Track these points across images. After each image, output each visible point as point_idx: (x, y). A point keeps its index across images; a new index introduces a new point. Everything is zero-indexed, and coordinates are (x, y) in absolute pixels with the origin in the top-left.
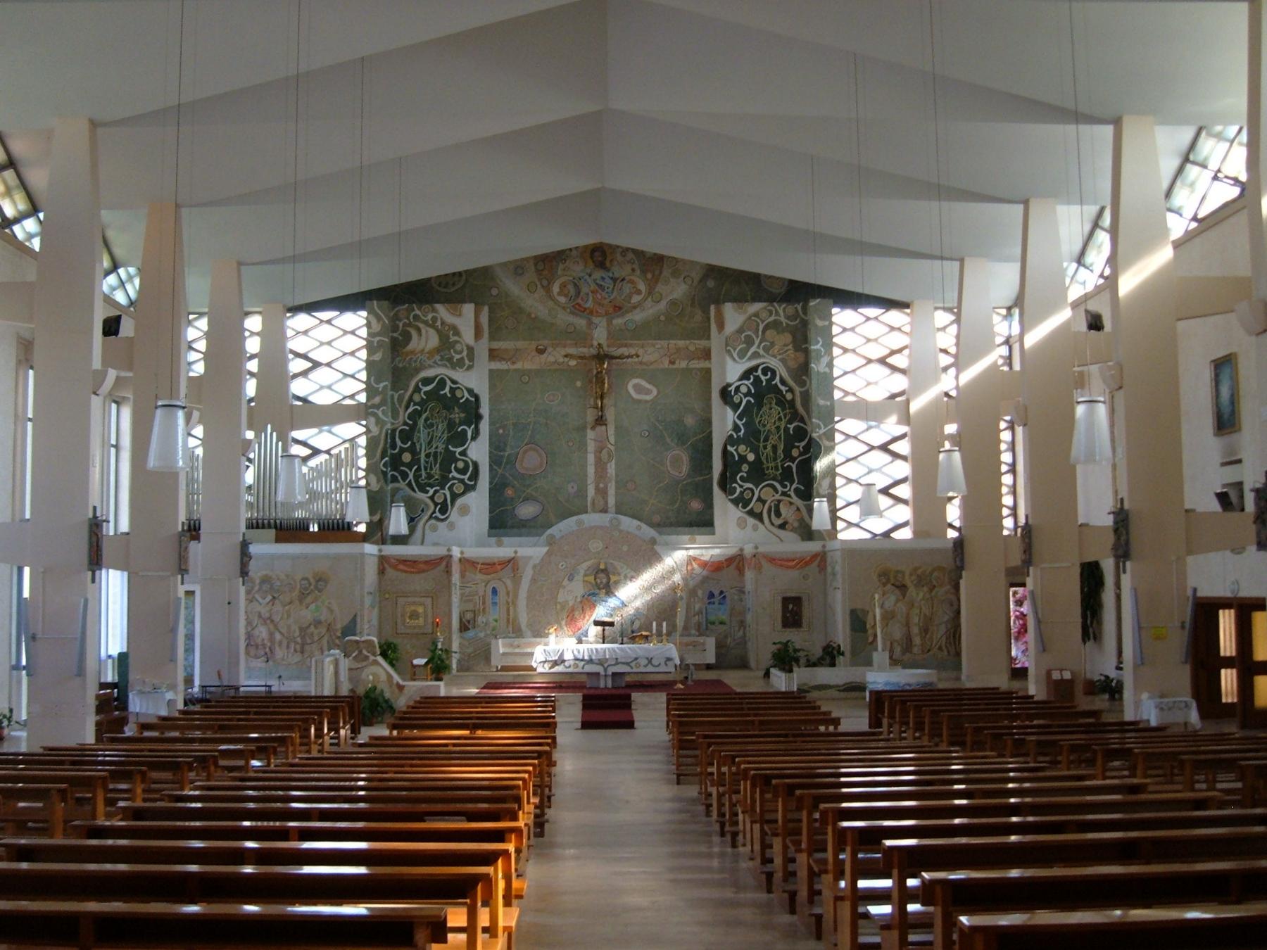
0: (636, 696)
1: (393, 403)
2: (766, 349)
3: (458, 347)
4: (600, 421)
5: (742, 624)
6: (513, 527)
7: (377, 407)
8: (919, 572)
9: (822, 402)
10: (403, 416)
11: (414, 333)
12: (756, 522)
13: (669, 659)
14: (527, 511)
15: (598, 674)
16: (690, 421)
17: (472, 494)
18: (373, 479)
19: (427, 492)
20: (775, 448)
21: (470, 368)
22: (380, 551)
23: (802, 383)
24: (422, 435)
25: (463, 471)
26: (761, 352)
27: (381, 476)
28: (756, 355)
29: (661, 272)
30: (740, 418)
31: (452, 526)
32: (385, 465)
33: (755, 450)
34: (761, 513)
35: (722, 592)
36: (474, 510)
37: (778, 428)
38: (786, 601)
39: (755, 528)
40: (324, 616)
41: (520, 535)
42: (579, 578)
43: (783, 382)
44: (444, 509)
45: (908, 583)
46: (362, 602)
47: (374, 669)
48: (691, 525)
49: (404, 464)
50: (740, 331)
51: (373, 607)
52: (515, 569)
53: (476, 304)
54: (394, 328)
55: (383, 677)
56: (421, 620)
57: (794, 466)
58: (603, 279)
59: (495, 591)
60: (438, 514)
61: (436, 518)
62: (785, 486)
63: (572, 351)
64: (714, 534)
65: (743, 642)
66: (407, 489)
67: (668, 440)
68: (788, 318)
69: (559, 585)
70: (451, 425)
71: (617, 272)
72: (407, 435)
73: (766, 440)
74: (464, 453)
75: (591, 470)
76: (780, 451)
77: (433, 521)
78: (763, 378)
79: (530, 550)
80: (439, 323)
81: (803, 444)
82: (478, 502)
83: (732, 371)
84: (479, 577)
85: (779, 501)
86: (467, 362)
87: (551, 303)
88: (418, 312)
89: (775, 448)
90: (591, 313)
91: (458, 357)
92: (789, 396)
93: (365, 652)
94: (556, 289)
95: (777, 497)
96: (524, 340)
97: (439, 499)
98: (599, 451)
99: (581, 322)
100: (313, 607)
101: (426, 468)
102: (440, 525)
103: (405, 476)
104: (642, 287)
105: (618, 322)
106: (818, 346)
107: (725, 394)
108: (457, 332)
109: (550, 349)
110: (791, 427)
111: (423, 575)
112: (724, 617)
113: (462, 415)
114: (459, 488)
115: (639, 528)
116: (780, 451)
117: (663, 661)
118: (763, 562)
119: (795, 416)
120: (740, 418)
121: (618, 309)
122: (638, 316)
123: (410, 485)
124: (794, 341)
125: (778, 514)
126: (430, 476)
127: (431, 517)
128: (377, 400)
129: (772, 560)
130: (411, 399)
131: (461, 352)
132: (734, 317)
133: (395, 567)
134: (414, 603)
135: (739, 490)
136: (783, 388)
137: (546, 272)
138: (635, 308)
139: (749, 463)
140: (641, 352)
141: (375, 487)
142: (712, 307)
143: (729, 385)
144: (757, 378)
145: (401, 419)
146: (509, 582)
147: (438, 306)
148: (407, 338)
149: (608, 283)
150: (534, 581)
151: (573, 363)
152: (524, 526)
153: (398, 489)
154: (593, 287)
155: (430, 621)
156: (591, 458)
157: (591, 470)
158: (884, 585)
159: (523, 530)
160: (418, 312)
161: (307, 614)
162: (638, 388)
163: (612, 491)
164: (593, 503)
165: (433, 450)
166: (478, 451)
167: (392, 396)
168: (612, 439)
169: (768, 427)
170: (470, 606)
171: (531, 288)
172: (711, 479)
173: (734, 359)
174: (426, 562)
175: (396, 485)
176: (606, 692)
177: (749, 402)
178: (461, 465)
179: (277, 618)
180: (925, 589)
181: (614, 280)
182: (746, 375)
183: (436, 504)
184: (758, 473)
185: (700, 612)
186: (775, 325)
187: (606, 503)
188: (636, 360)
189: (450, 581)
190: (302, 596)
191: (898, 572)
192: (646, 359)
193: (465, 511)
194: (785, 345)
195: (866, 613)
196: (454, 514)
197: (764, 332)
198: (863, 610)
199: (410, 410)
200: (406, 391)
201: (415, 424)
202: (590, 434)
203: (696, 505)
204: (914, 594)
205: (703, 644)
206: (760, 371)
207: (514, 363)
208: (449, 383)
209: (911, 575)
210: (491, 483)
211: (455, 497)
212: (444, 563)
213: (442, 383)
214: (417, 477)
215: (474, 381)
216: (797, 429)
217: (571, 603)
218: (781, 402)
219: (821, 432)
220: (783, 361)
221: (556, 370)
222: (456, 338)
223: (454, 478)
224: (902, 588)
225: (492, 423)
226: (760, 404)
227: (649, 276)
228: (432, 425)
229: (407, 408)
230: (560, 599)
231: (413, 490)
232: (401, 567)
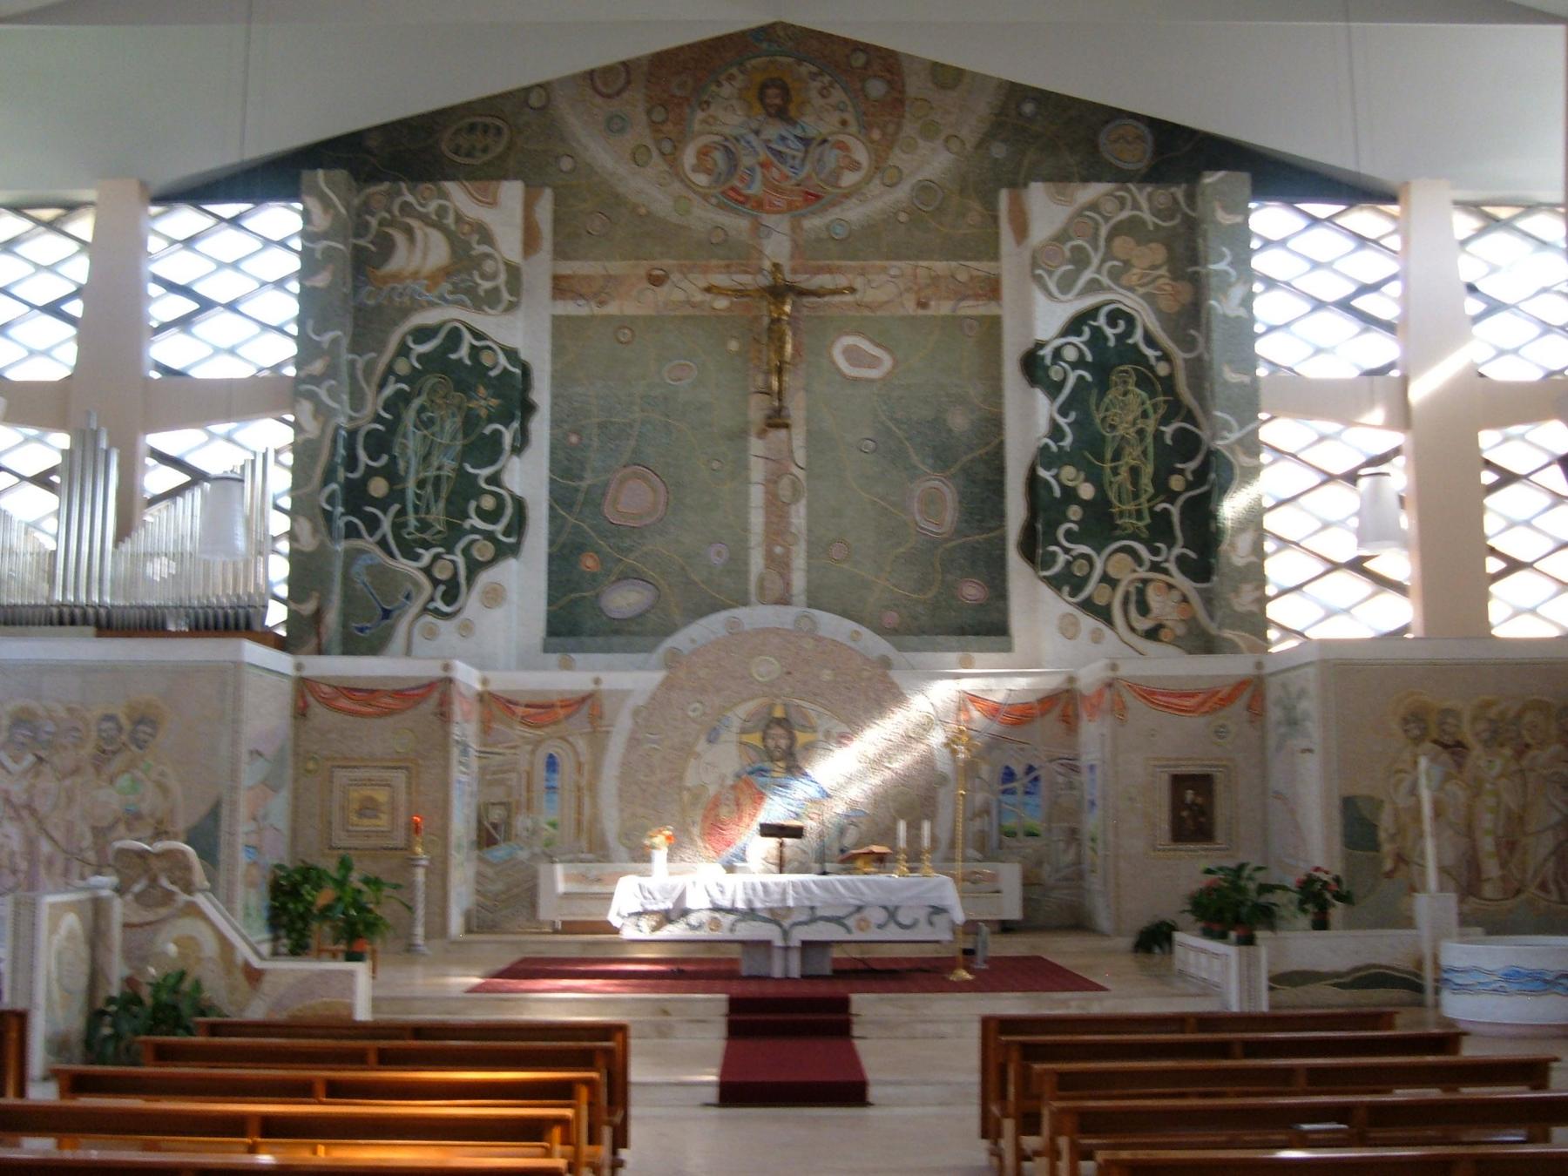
0: (865, 1005)
1: (353, 377)
2: (1115, 275)
3: (489, 266)
4: (777, 420)
5: (1073, 835)
6: (594, 633)
7: (316, 380)
8: (1493, 713)
9: (1231, 376)
10: (374, 403)
11: (400, 238)
12: (1101, 625)
13: (938, 910)
14: (624, 600)
15: (766, 944)
16: (959, 421)
17: (510, 566)
18: (305, 527)
19: (417, 557)
20: (1135, 472)
21: (512, 307)
22: (299, 667)
23: (1188, 344)
24: (411, 442)
25: (492, 516)
26: (1105, 281)
27: (321, 521)
28: (1094, 286)
29: (899, 126)
30: (1063, 411)
31: (467, 629)
32: (331, 499)
33: (1094, 477)
34: (1108, 608)
35: (1030, 769)
36: (513, 596)
37: (1141, 432)
39: (1097, 638)
40: (149, 801)
41: (609, 650)
42: (730, 737)
43: (1150, 340)
44: (451, 595)
45: (1469, 739)
46: (234, 773)
47: (187, 926)
48: (962, 631)
49: (375, 502)
50: (1061, 237)
51: (270, 784)
52: (596, 717)
53: (527, 186)
54: (361, 229)
55: (210, 947)
56: (383, 822)
57: (1175, 511)
58: (783, 139)
59: (552, 764)
60: (439, 604)
61: (438, 613)
62: (1155, 551)
63: (721, 280)
64: (1008, 648)
65: (1077, 876)
66: (379, 553)
67: (915, 459)
68: (1156, 212)
69: (686, 751)
70: (470, 422)
71: (812, 125)
72: (379, 443)
73: (1117, 456)
74: (494, 480)
75: (757, 519)
76: (1146, 481)
77: (429, 618)
78: (1109, 332)
79: (627, 679)
80: (450, 221)
81: (1192, 465)
82: (522, 581)
83: (1047, 318)
84: (520, 731)
85: (1145, 582)
86: (506, 296)
87: (677, 186)
88: (410, 198)
89: (1135, 472)
90: (759, 205)
91: (487, 285)
92: (1162, 369)
93: (165, 882)
94: (689, 157)
95: (1142, 573)
96: (624, 258)
97: (442, 573)
98: (772, 482)
99: (737, 224)
100: (124, 781)
101: (417, 509)
102: (442, 624)
103: (373, 524)
104: (861, 154)
105: (814, 223)
106: (1222, 266)
107: (1032, 366)
108: (486, 237)
109: (675, 277)
110: (1168, 430)
111: (390, 720)
112: (1035, 821)
113: (494, 402)
114: (484, 550)
115: (855, 636)
116: (1146, 481)
117: (922, 915)
118: (1129, 698)
119: (1175, 408)
120: (1063, 411)
121: (812, 198)
122: (854, 213)
123: (382, 543)
124: (1171, 260)
125: (1144, 609)
126: (424, 526)
127: (425, 610)
128: (318, 367)
129: (1148, 694)
130: (390, 370)
131: (493, 277)
132: (1047, 210)
133: (327, 703)
134: (370, 782)
135: (1062, 558)
136: (1150, 353)
137: (669, 127)
138: (847, 196)
139: (1084, 504)
140: (858, 283)
141: (308, 543)
142: (1004, 196)
143: (1040, 345)
144: (1097, 332)
145: (368, 410)
146: (582, 744)
147: (451, 186)
148: (386, 247)
149: (794, 149)
150: (634, 741)
151: (722, 303)
152: (616, 632)
153: (361, 552)
154: (764, 155)
155: (402, 820)
156: (757, 495)
157: (757, 519)
158: (1417, 741)
159: (616, 640)
160: (410, 198)
161: (110, 798)
162: (853, 355)
163: (799, 561)
164: (761, 588)
165: (431, 473)
166: (526, 475)
167: (352, 364)
168: (800, 456)
169: (1120, 432)
170: (499, 794)
171: (638, 157)
172: (1003, 539)
173: (1050, 295)
174: (398, 694)
175: (358, 543)
176: (789, 990)
177: (1081, 378)
178: (488, 503)
179: (43, 806)
180: (1507, 751)
181: (806, 141)
182: (1074, 326)
183: (436, 582)
184: (1100, 524)
185: (986, 811)
186: (1132, 228)
187: (788, 585)
188: (848, 298)
189: (447, 735)
190: (103, 756)
191: (1447, 712)
192: (870, 296)
193: (495, 596)
194: (1154, 267)
195: (1377, 804)
196: (472, 603)
197: (1110, 238)
198: (1371, 799)
199: (389, 391)
200: (380, 352)
201: (398, 418)
202: (756, 446)
203: (972, 591)
204: (1482, 763)
205: (993, 878)
206: (1101, 321)
207: (602, 303)
208: (468, 338)
209: (1475, 719)
210: (551, 543)
211: (475, 567)
213: (454, 337)
214: (398, 527)
215: (521, 332)
216: (1180, 434)
217: (712, 790)
218: (1147, 381)
219: (1233, 437)
220: (1150, 298)
221: (685, 318)
222: (485, 249)
223: (474, 530)
224: (1456, 748)
225: (555, 423)
226: (1103, 385)
227: (876, 135)
228: (430, 422)
229: (382, 385)
230: (690, 780)
231: (391, 555)
232: (344, 703)
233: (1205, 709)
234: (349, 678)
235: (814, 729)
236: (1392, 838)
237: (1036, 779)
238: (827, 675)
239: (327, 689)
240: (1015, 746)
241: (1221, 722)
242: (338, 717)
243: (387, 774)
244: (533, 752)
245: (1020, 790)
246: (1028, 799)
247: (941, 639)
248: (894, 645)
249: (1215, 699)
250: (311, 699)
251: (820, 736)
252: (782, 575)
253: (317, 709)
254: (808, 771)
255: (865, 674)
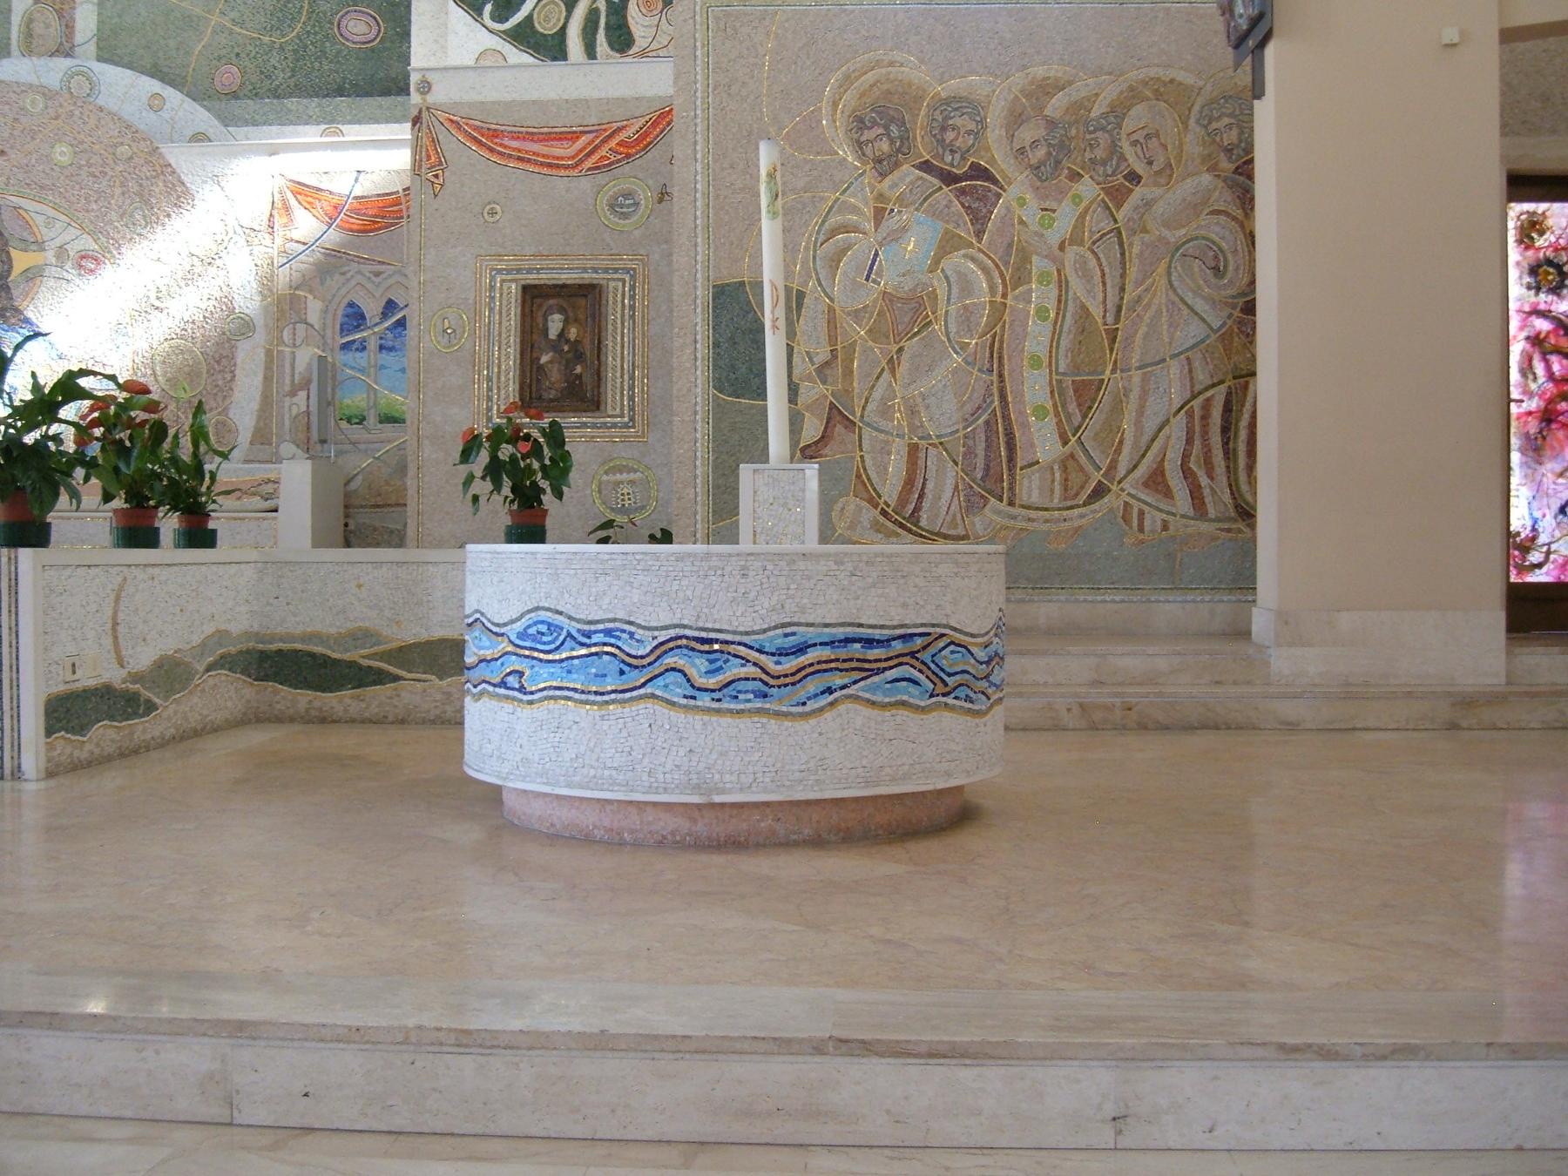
8: (1056, 106)
35: (390, 306)
38: (534, 296)
45: (1000, 159)
115: (156, 103)
118: (451, 144)
158: (884, 166)
164: (28, 35)
180: (1088, 189)
187: (69, 28)
191: (955, 103)
204: (1031, 212)
209: (1016, 119)
224: (972, 183)
233: (589, 164)
235: (40, 246)
236: (823, 370)
237: (401, 323)
238: (62, 154)
240: (366, 269)
241: (625, 186)
245: (373, 344)
246: (386, 358)
247: (291, 103)
248: (218, 117)
249: (613, 143)
251: (50, 255)
252: (60, 14)
254: (29, 314)
255: (123, 150)
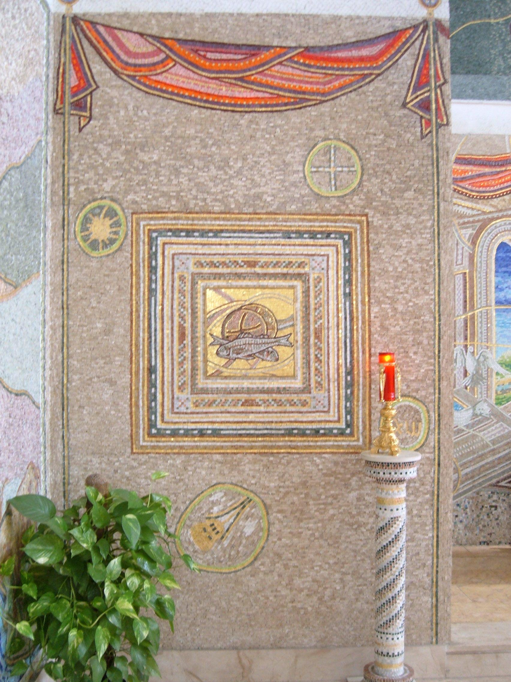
111: (295, 117)
133: (142, 77)
134: (250, 269)
155: (335, 361)
174: (310, 55)
212: (407, 62)
232: (179, 76)
234: (190, 19)
239: (133, 43)
242: (171, 110)
243: (294, 249)
244: (474, 241)
250: (98, 67)
253: (112, 91)
